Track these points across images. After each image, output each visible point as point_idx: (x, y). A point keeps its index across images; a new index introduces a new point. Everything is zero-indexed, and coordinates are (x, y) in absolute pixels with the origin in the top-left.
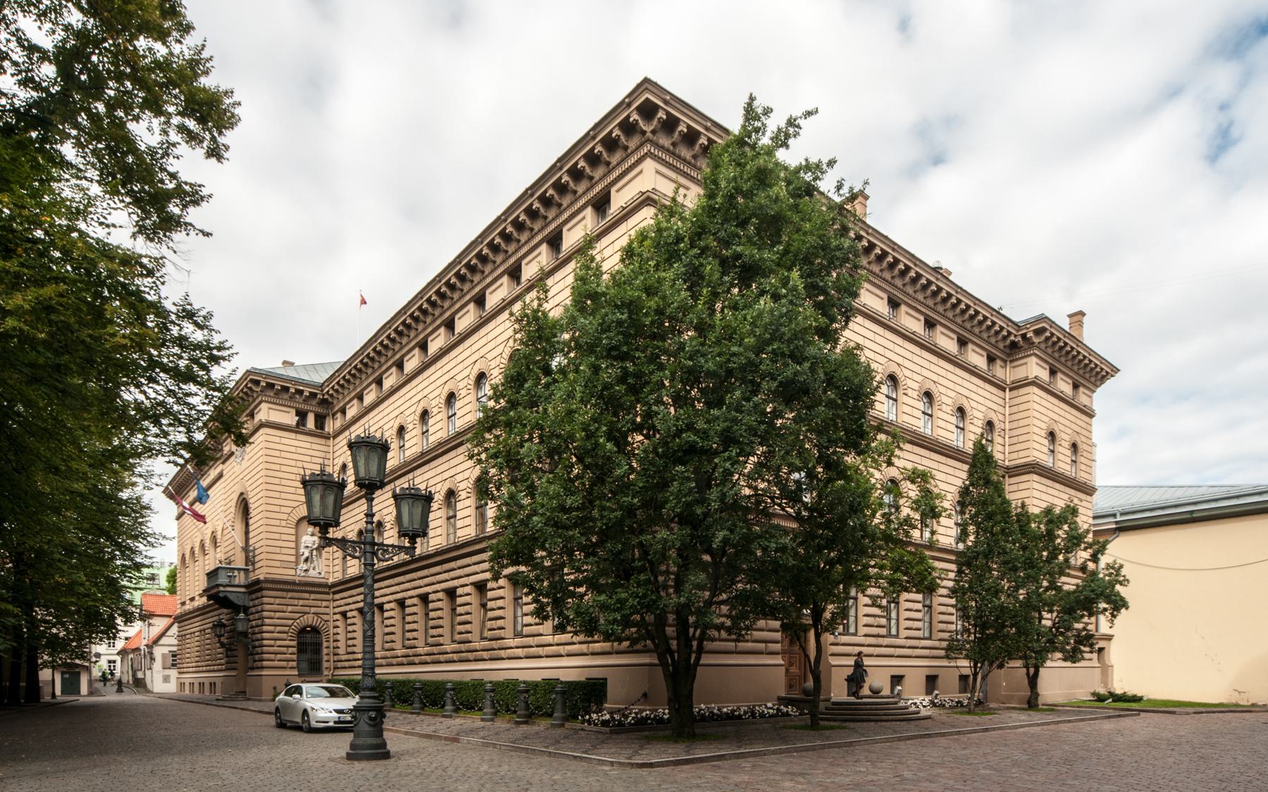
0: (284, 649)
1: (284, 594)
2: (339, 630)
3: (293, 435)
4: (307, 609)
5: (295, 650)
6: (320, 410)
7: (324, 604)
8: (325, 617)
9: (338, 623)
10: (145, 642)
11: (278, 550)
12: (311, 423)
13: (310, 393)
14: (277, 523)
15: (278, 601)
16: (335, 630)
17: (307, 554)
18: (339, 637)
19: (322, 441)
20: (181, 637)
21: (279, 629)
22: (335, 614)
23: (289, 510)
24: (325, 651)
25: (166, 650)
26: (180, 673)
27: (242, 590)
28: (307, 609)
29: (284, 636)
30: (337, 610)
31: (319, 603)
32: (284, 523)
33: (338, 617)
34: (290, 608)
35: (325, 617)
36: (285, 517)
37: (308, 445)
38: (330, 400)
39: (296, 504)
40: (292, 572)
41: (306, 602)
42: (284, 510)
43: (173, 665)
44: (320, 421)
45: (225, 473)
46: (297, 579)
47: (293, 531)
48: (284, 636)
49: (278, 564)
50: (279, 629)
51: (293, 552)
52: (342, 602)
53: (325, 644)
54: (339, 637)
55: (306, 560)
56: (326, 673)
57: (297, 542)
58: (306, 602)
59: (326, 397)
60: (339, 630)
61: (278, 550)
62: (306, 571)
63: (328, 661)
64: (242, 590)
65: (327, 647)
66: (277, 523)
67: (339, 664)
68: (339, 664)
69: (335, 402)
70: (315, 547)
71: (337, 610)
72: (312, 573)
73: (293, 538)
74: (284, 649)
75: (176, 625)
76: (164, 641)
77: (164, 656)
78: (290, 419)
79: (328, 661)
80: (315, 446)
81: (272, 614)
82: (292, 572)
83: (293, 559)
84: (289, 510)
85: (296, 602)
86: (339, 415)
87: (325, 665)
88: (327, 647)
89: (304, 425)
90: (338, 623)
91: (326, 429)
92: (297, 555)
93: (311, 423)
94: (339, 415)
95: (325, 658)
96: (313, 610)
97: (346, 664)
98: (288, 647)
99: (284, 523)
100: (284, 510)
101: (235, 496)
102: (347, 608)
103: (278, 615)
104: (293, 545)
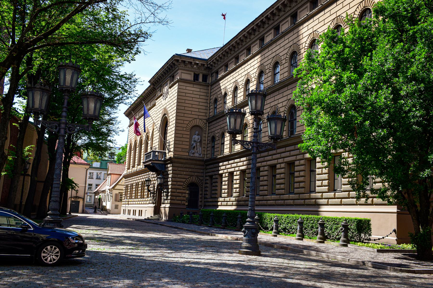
0: (180, 194)
1: (183, 165)
2: (208, 185)
3: (192, 85)
6: (205, 72)
7: (201, 171)
8: (201, 178)
9: (208, 181)
11: (181, 143)
12: (200, 80)
13: (201, 64)
14: (181, 129)
16: (206, 185)
18: (208, 189)
19: (205, 88)
21: (179, 183)
22: (206, 176)
23: (187, 122)
24: (200, 196)
25: (117, 192)
29: (181, 187)
30: (207, 174)
32: (185, 129)
33: (208, 178)
34: (185, 173)
35: (201, 178)
36: (185, 126)
37: (198, 90)
38: (211, 67)
39: (191, 119)
40: (187, 154)
41: (193, 170)
42: (185, 122)
44: (205, 78)
45: (157, 104)
46: (189, 157)
47: (189, 133)
48: (181, 187)
49: (180, 150)
50: (179, 183)
51: (188, 143)
52: (210, 170)
53: (200, 193)
54: (208, 189)
56: (200, 208)
57: (191, 138)
58: (193, 170)
59: (209, 66)
60: (208, 185)
61: (181, 143)
62: (193, 153)
63: (201, 202)
65: (201, 194)
66: (181, 129)
67: (207, 204)
68: (207, 204)
69: (213, 68)
70: (198, 141)
71: (207, 174)
72: (197, 155)
73: (188, 136)
74: (180, 194)
77: (116, 194)
78: (189, 77)
79: (201, 202)
80: (202, 90)
81: (176, 175)
82: (187, 154)
83: (188, 147)
84: (187, 122)
86: (214, 74)
87: (200, 204)
88: (201, 194)
89: (197, 80)
90: (208, 181)
91: (208, 82)
92: (191, 145)
93: (200, 80)
94: (214, 74)
95: (200, 200)
96: (196, 174)
97: (211, 204)
99: (185, 129)
100: (185, 122)
101: (161, 116)
102: (213, 173)
103: (179, 176)
104: (188, 140)
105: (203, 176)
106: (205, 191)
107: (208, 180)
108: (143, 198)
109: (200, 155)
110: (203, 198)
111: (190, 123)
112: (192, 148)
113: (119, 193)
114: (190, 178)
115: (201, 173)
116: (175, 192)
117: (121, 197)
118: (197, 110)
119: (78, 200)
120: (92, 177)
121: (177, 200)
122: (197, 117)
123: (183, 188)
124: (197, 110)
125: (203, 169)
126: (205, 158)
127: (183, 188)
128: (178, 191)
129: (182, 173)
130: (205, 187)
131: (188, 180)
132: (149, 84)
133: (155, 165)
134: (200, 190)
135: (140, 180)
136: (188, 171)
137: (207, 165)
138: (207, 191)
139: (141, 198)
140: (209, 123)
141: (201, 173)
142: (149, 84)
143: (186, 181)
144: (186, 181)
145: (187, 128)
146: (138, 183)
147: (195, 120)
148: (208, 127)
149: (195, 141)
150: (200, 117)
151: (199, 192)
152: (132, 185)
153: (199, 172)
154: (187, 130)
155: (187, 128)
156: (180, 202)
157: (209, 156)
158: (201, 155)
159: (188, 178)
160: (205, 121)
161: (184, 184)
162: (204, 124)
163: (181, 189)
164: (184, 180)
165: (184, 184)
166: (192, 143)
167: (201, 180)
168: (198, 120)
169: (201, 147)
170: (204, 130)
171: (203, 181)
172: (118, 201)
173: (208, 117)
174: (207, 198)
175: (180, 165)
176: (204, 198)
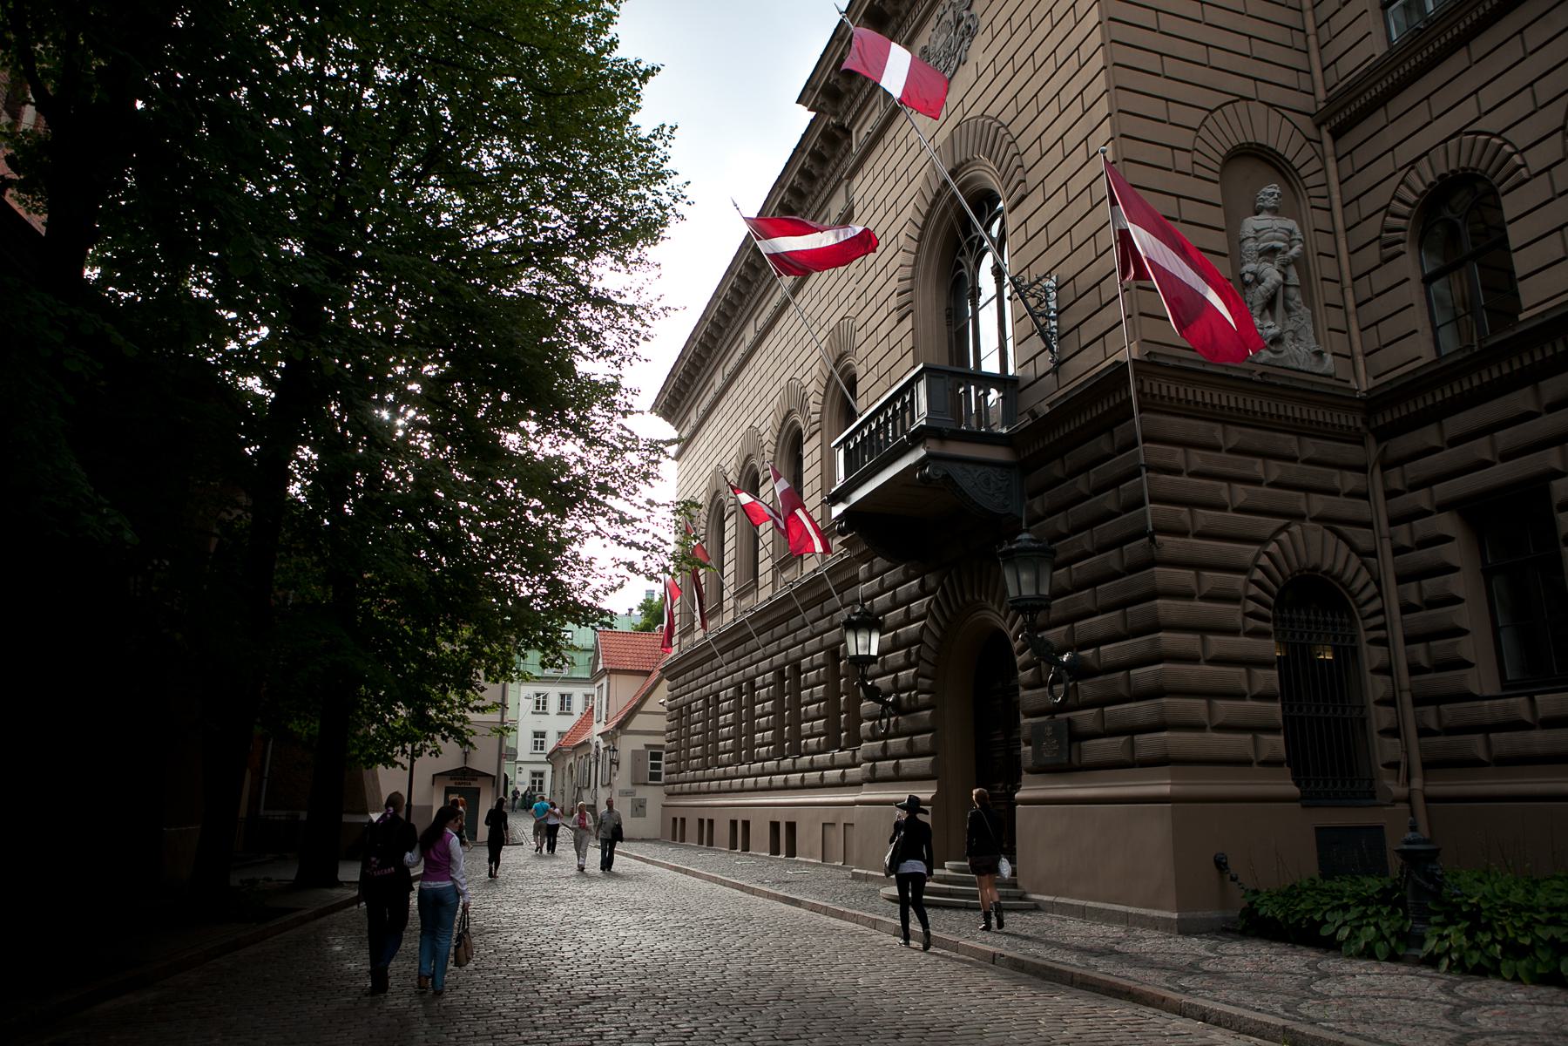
1: (1217, 432)
4: (1298, 501)
5: (1268, 678)
7: (1352, 480)
8: (1362, 538)
9: (1450, 553)
10: (599, 728)
14: (1163, 156)
15: (1197, 459)
17: (1272, 274)
20: (679, 713)
23: (1195, 118)
24: (1377, 686)
25: (638, 743)
26: (670, 794)
27: (999, 454)
28: (1298, 501)
29: (1231, 613)
31: (1337, 479)
32: (1184, 161)
33: (1445, 523)
34: (1241, 493)
35: (1362, 538)
36: (1185, 139)
39: (1213, 100)
41: (1294, 471)
42: (1179, 114)
43: (655, 777)
48: (1231, 613)
50: (1212, 579)
53: (1373, 656)
55: (1270, 304)
58: (1294, 471)
64: (999, 454)
65: (1385, 670)
66: (1163, 156)
71: (1421, 498)
75: (666, 683)
76: (638, 723)
77: (635, 753)
79: (1393, 732)
84: (1194, 117)
85: (1258, 467)
88: (1385, 670)
95: (1382, 717)
96: (1319, 504)
98: (1249, 663)
99: (1184, 161)
100: (1179, 114)
103: (1205, 517)
105: (1369, 525)
106: (1409, 640)
107: (1445, 539)
108: (797, 751)
109: (1319, 354)
110: (1407, 698)
111: (1209, 123)
112: (1259, 302)
113: (646, 746)
114: (1283, 537)
115: (1350, 495)
116: (1192, 659)
117: (654, 766)
118: (1242, 45)
119: (474, 785)
120: (544, 708)
121: (1222, 728)
122: (1246, 88)
123: (1253, 623)
124: (1242, 45)
125: (1362, 469)
126: (1363, 383)
127: (1253, 623)
128: (1217, 644)
129: (1223, 490)
130: (1407, 608)
131: (1273, 547)
132: (805, 116)
133: (957, 471)
134: (1364, 636)
135: (764, 664)
136: (1257, 482)
137: (1383, 434)
138: (1461, 632)
139: (780, 754)
140: (1337, 134)
141: (1350, 495)
142: (805, 116)
143: (1264, 560)
144: (1264, 560)
145: (1197, 157)
146: (751, 681)
147: (1241, 105)
148: (1338, 160)
149: (1272, 251)
150: (1272, 94)
151: (1355, 651)
152: (712, 700)
153: (1335, 493)
154: (1199, 171)
155: (1197, 157)
156: (1239, 743)
157: (1408, 348)
158: (1329, 358)
159: (1273, 537)
160: (1305, 123)
161: (1254, 590)
162: (1298, 140)
163: (1234, 632)
164: (1248, 552)
165: (1254, 590)
166: (1251, 267)
167: (1362, 554)
168: (1258, 110)
169: (1309, 301)
170: (1309, 182)
171: (1372, 560)
172: (646, 784)
173: (1321, 95)
174: (1469, 697)
175: (1200, 429)
176: (1419, 701)
